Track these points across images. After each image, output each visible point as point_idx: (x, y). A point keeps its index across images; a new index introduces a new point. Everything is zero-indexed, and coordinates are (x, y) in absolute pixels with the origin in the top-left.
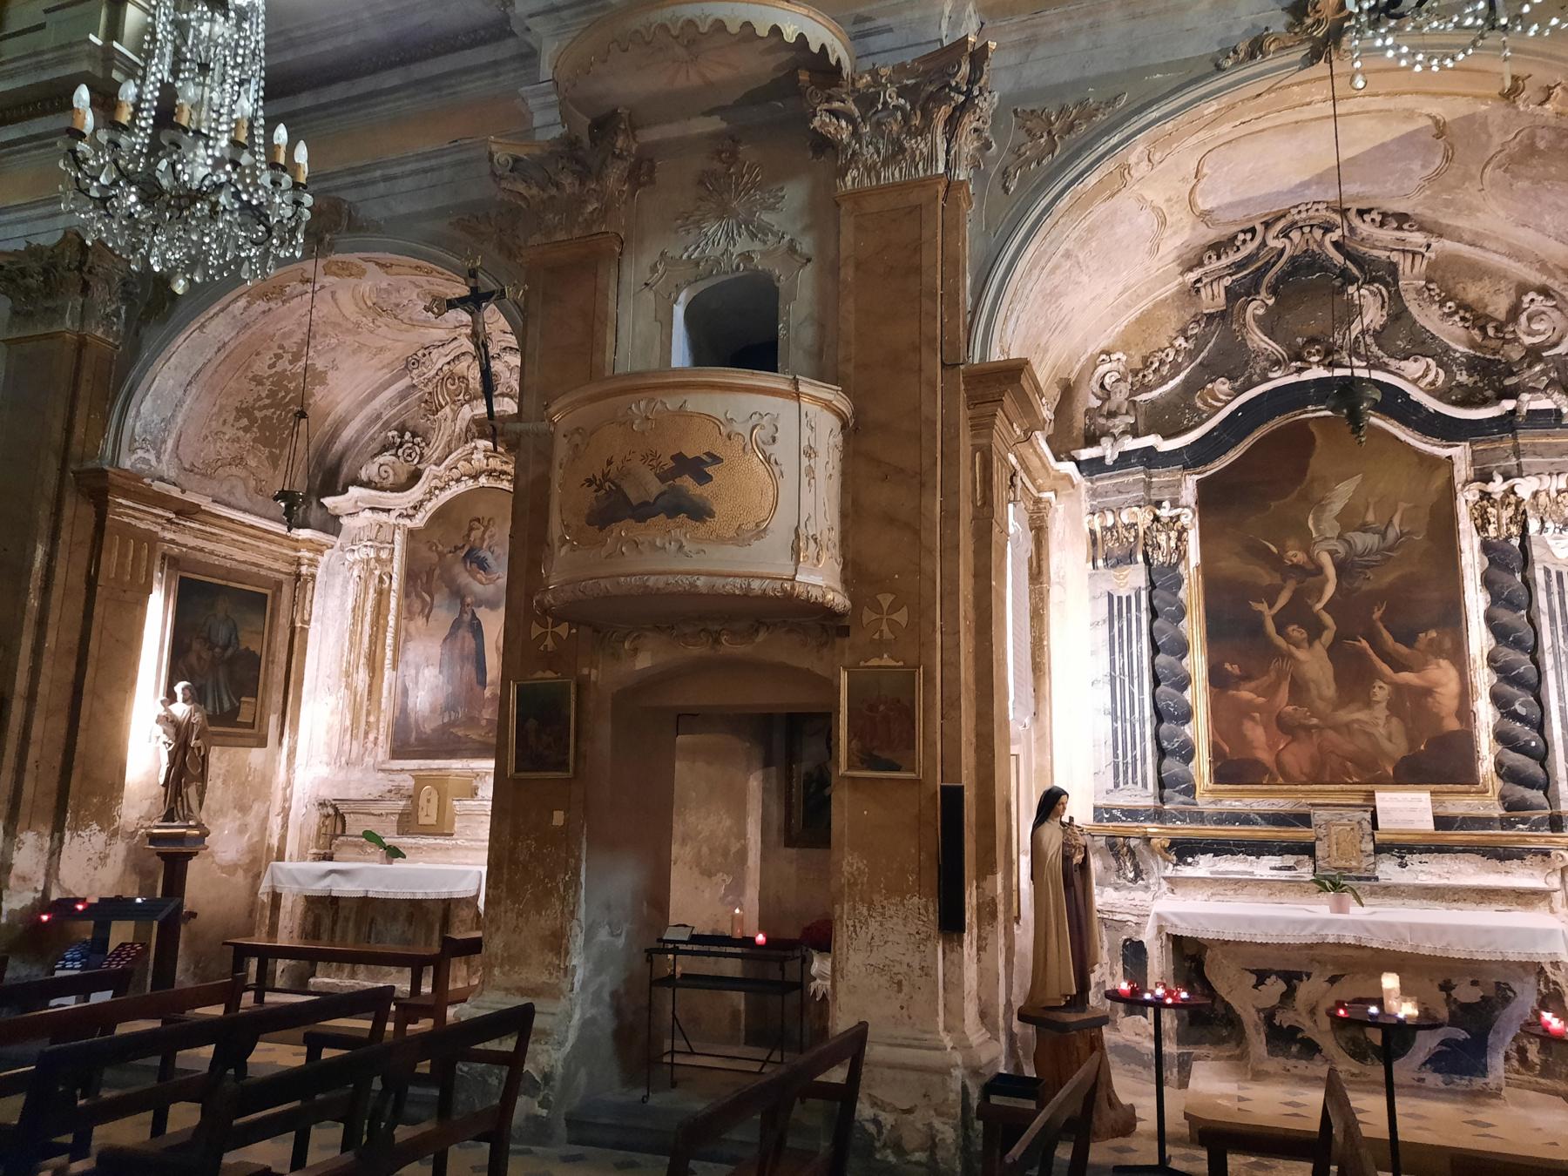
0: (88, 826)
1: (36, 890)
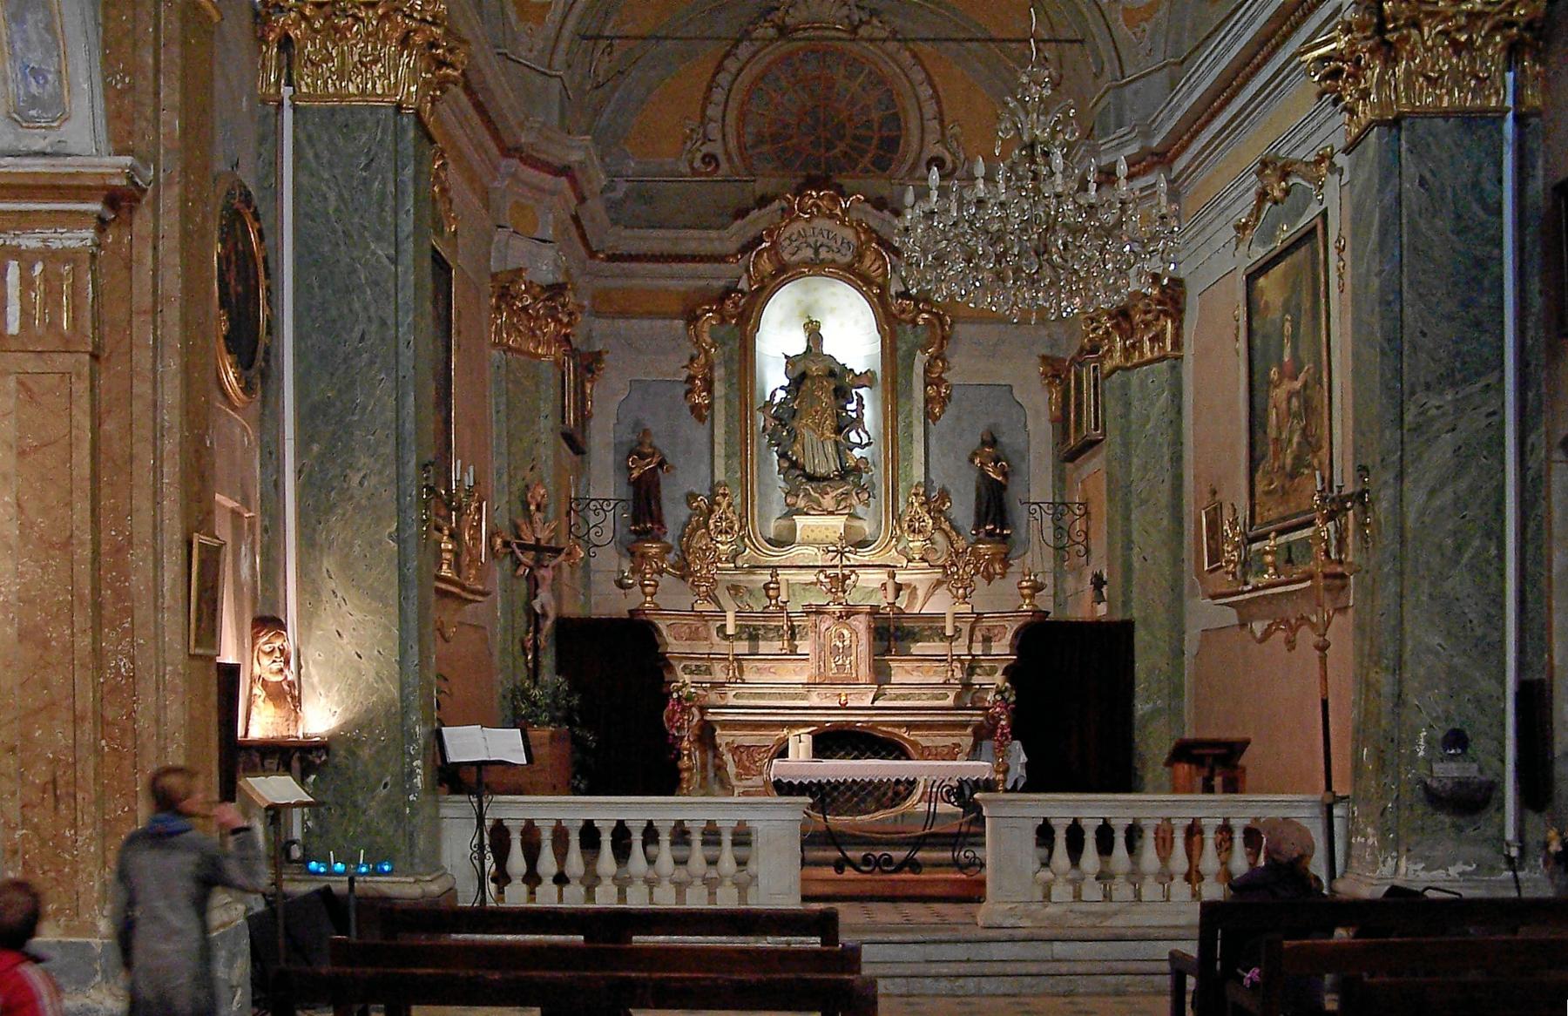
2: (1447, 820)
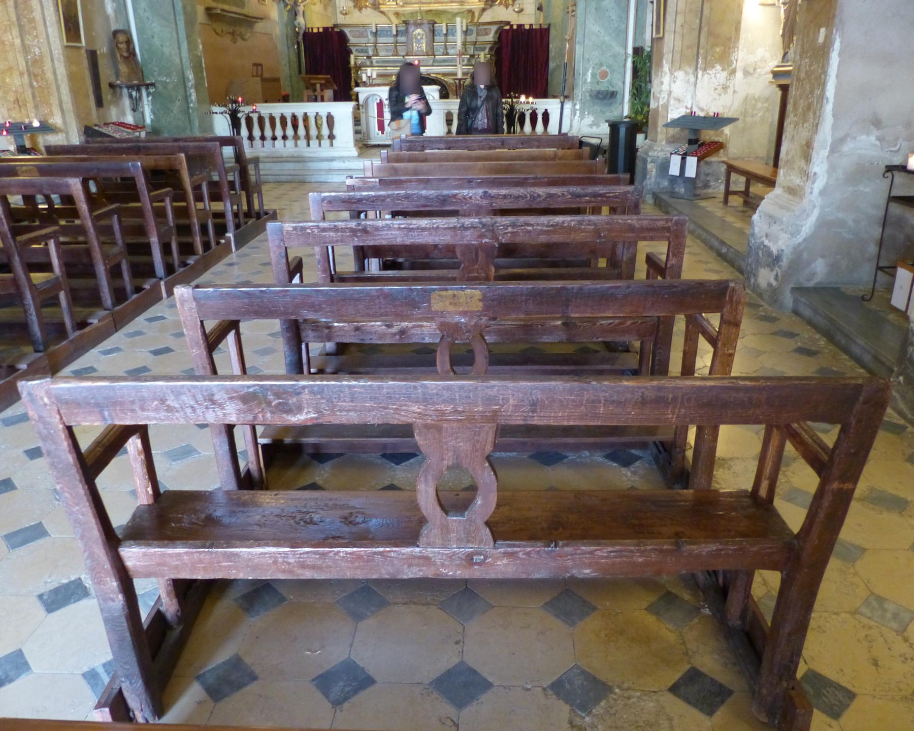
0: (713, 67)
1: (687, 108)
2: (599, 109)
